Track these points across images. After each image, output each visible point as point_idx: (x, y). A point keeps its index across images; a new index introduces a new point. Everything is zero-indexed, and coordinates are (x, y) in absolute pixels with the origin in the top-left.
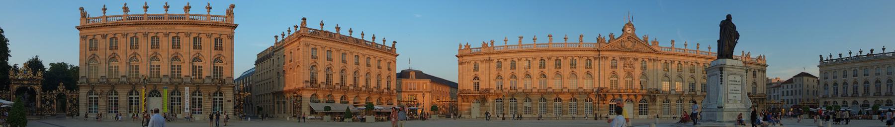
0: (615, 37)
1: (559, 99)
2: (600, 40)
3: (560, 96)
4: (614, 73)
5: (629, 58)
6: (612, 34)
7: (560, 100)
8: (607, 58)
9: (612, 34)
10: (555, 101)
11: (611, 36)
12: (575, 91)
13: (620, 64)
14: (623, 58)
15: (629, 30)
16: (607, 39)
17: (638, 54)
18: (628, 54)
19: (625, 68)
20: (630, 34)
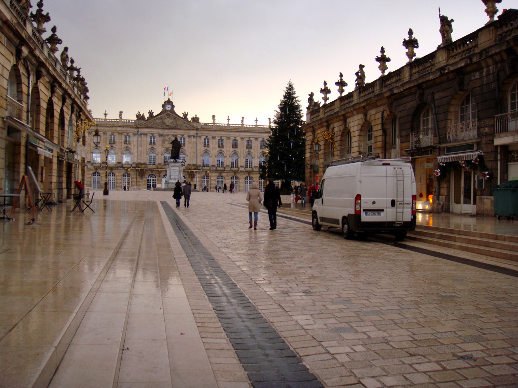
0: (155, 115)
1: (98, 173)
2: (140, 117)
3: (99, 171)
4: (152, 149)
5: (168, 135)
6: (151, 111)
7: (99, 174)
8: (145, 134)
9: (151, 111)
10: (93, 175)
11: (151, 113)
12: (114, 166)
13: (158, 140)
14: (162, 135)
15: (168, 107)
16: (147, 116)
17: (176, 131)
18: (166, 131)
19: (164, 144)
20: (169, 111)
